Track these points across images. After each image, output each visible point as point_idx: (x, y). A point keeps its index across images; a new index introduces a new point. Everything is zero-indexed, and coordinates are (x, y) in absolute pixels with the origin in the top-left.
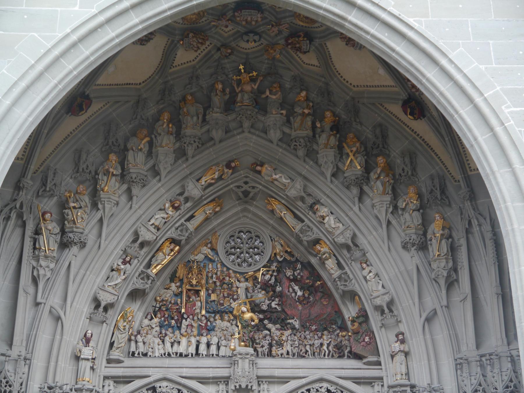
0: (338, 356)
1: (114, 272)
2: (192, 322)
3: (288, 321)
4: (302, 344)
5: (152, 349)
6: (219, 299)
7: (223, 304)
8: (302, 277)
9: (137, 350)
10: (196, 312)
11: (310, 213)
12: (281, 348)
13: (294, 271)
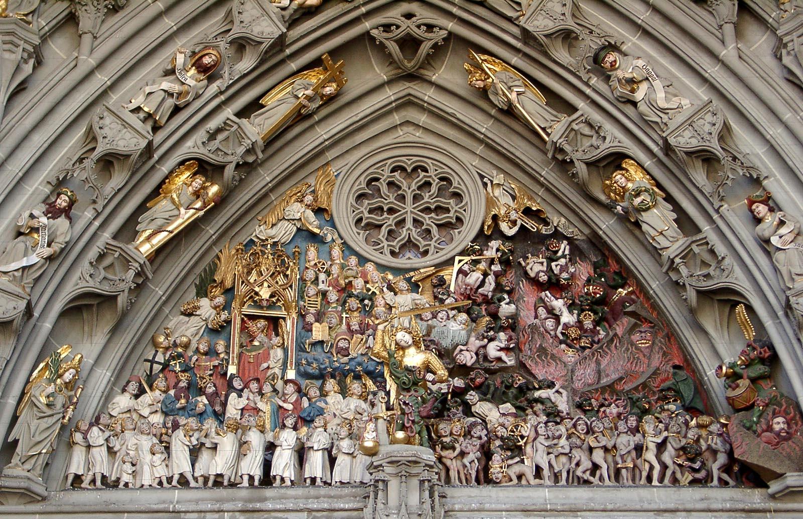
0: (690, 478)
1: (21, 238)
3: (537, 394)
4: (580, 447)
5: (133, 465)
7: (347, 349)
8: (573, 276)
9: (89, 470)
11: (594, 81)
12: (517, 459)
13: (551, 260)
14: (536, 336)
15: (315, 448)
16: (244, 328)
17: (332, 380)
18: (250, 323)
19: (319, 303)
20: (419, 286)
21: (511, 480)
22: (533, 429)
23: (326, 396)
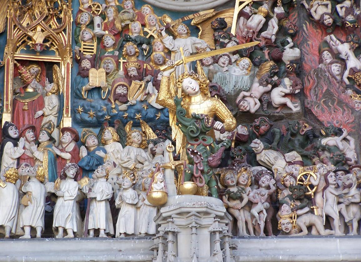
2: (34, 147)
3: (324, 141)
6: (114, 83)
7: (125, 96)
10: (45, 120)
12: (307, 209)
14: (322, 82)
15: (98, 199)
16: (17, 74)
17: (110, 128)
18: (23, 70)
19: (95, 48)
20: (198, 30)
21: (301, 231)
22: (323, 178)
23: (105, 144)
